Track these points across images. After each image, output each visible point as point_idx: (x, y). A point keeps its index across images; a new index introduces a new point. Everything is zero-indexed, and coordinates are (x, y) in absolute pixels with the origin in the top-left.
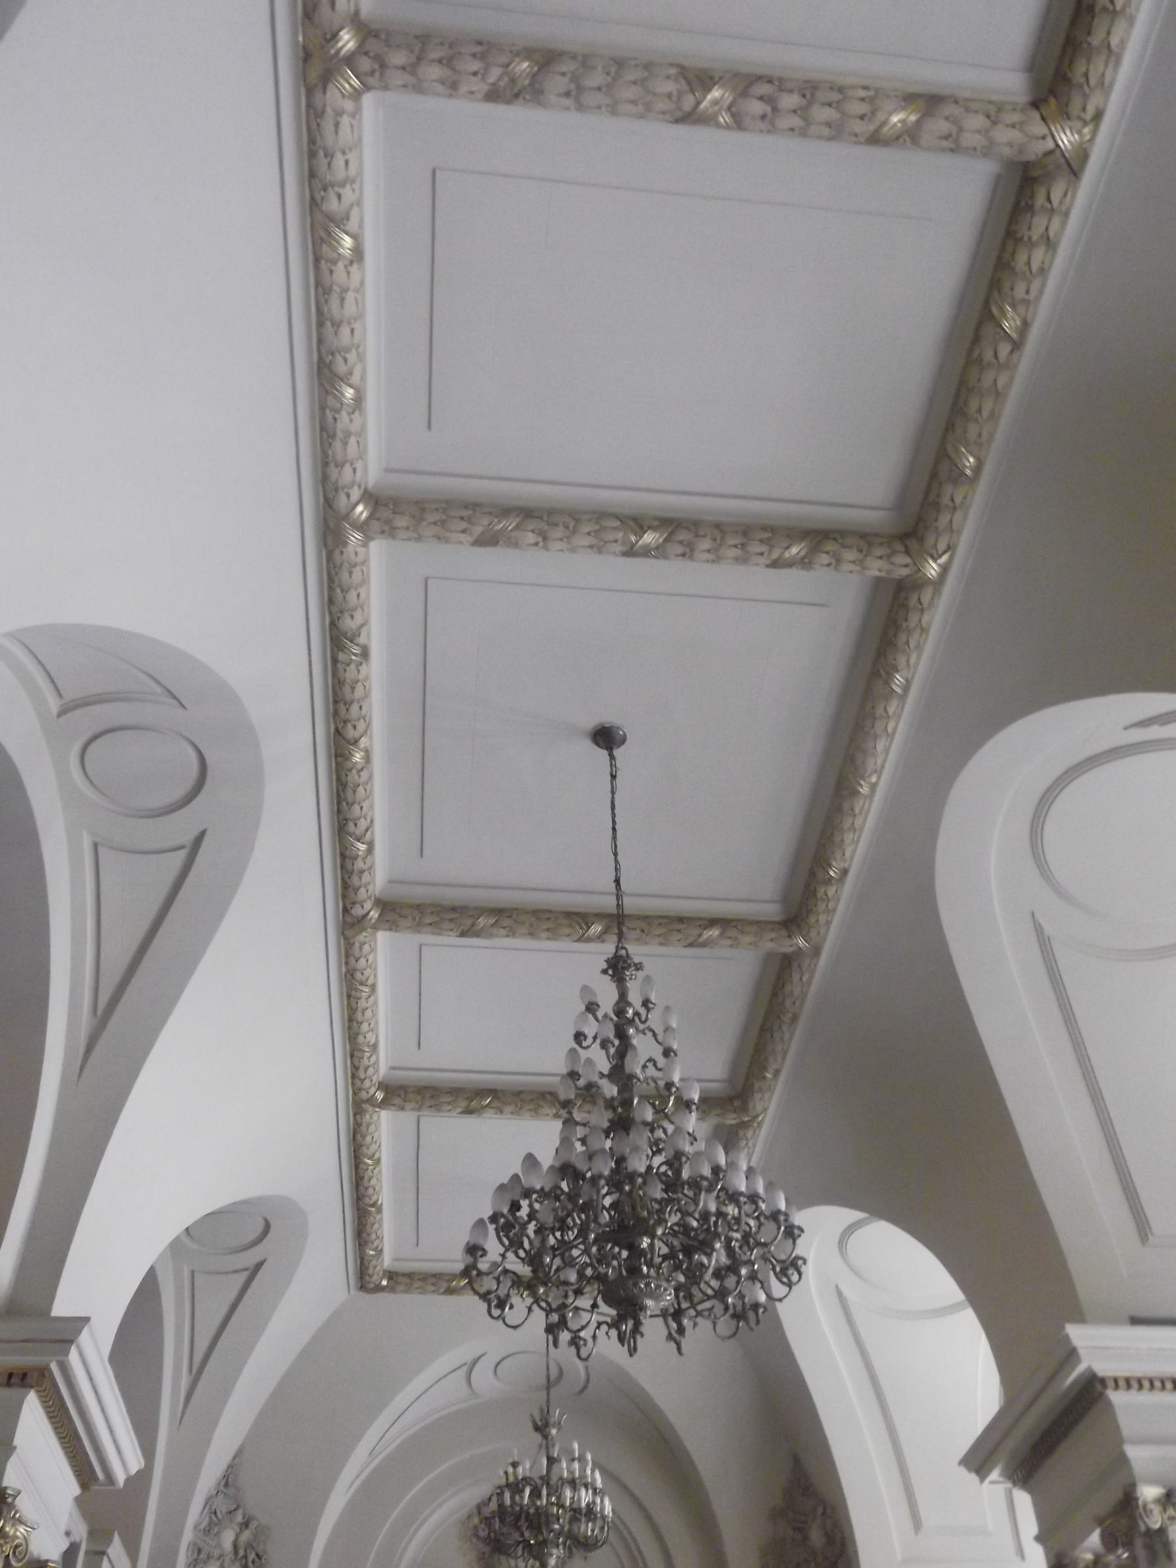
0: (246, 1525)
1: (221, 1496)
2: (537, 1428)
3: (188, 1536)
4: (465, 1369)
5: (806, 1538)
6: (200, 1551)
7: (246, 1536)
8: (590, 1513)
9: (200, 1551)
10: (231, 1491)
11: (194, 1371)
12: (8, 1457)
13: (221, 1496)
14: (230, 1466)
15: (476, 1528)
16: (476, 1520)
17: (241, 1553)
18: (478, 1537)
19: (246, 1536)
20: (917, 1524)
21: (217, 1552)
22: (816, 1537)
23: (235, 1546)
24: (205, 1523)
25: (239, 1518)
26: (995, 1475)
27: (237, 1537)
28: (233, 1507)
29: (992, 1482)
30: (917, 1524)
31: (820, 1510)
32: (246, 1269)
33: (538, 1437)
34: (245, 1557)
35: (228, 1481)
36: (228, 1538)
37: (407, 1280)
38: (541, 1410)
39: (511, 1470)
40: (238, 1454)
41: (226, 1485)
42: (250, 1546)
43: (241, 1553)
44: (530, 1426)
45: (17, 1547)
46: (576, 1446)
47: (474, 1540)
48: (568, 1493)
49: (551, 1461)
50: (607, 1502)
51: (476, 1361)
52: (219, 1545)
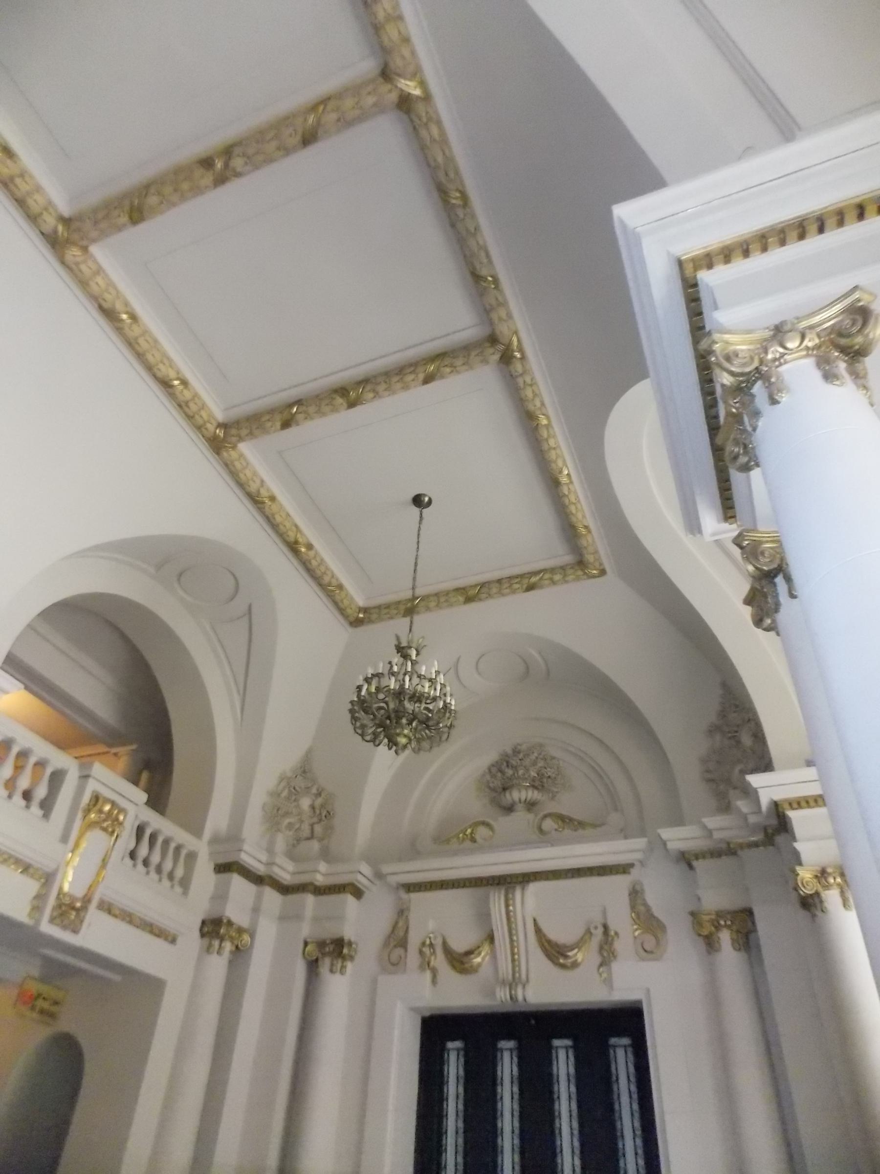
0: (319, 794)
4: (452, 671)
5: (738, 742)
6: (278, 810)
9: (278, 810)
13: (300, 778)
15: (488, 782)
16: (488, 777)
17: (318, 812)
18: (490, 788)
19: (319, 801)
22: (747, 740)
23: (313, 807)
24: (285, 793)
25: (314, 791)
27: (314, 801)
32: (245, 615)
34: (320, 814)
35: (304, 770)
36: (305, 803)
37: (377, 610)
42: (322, 806)
43: (318, 812)
47: (487, 790)
52: (298, 806)
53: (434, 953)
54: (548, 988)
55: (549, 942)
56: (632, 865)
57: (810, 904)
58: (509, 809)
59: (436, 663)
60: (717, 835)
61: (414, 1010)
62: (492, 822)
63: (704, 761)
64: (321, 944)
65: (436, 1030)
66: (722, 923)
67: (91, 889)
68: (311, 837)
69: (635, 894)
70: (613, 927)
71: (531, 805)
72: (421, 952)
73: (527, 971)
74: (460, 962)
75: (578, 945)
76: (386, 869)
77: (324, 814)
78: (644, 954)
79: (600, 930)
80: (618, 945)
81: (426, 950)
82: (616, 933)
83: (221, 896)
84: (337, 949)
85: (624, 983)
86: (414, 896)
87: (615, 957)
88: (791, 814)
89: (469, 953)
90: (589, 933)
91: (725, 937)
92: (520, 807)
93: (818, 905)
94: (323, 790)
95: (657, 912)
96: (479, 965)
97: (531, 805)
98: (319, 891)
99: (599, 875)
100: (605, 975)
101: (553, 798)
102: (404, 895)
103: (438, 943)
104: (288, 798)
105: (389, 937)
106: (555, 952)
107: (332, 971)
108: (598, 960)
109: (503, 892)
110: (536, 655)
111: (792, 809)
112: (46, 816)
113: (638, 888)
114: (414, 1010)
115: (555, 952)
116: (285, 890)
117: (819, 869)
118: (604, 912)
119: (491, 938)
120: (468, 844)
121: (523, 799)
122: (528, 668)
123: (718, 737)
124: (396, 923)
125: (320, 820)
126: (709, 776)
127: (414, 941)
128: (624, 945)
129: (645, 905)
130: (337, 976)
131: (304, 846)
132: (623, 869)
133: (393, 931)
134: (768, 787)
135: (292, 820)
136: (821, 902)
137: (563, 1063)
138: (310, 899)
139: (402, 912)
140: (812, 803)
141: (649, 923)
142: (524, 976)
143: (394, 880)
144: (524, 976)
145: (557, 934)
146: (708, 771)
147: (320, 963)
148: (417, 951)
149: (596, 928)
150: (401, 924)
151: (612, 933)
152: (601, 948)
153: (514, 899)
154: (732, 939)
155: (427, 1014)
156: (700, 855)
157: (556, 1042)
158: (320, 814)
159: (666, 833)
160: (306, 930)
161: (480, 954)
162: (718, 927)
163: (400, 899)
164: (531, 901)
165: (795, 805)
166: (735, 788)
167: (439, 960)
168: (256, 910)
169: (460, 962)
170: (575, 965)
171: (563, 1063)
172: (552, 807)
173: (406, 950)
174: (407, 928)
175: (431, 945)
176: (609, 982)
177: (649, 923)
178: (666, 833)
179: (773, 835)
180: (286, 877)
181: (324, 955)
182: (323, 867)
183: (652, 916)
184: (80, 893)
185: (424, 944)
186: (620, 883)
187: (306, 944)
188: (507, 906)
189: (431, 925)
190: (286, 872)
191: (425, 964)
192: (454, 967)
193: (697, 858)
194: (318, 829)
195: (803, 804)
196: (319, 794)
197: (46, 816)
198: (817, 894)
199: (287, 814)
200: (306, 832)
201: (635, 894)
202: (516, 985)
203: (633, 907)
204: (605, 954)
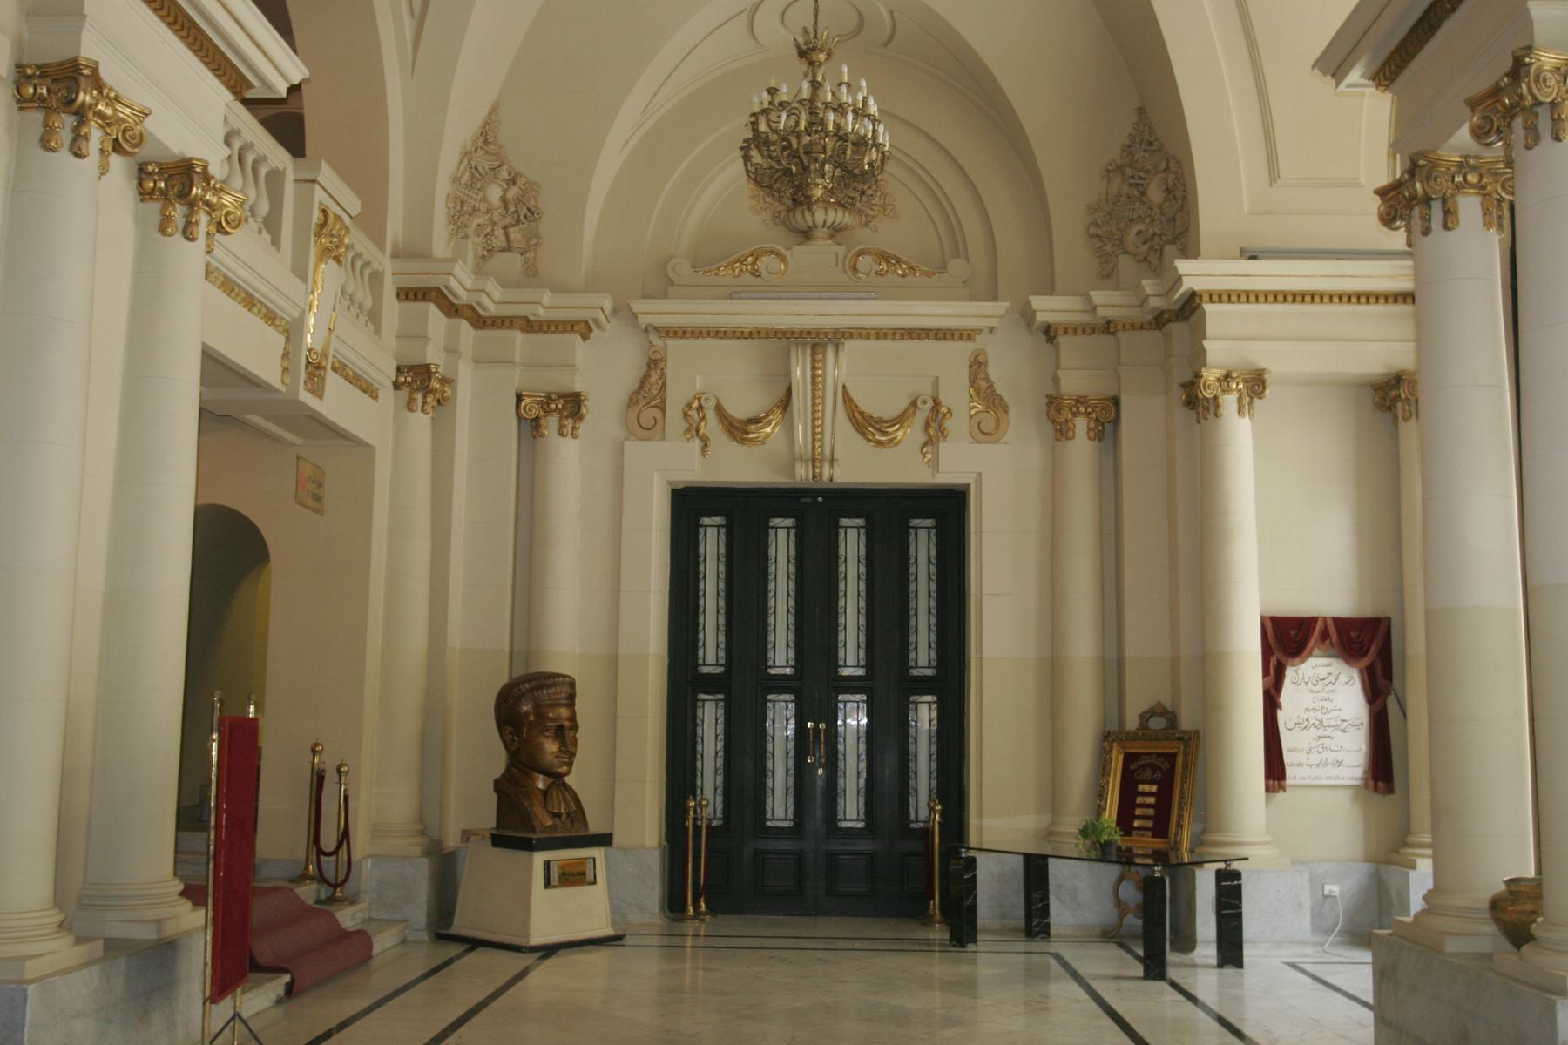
0: (512, 181)
1: (481, 153)
2: (802, 54)
3: (443, 187)
4: (745, 14)
5: (1143, 193)
6: (462, 204)
7: (513, 192)
8: (861, 143)
9: (462, 204)
10: (492, 148)
11: (417, 10)
12: (80, 29)
13: (481, 153)
14: (486, 124)
17: (512, 208)
19: (513, 192)
20: (1273, 174)
21: (483, 206)
22: (1155, 193)
23: (504, 200)
24: (465, 179)
25: (505, 175)
26: (1355, 75)
27: (505, 191)
28: (496, 164)
29: (1349, 86)
30: (1273, 174)
31: (1163, 165)
33: (803, 66)
34: (516, 211)
35: (486, 138)
36: (494, 193)
38: (806, 31)
39: (766, 95)
40: (494, 110)
41: (486, 142)
42: (518, 200)
43: (512, 208)
44: (795, 52)
45: (125, 131)
46: (845, 69)
48: (831, 117)
49: (816, 86)
50: (881, 129)
51: (756, 7)
52: (485, 199)
53: (703, 418)
54: (858, 465)
55: (862, 413)
56: (979, 331)
57: (1196, 403)
58: (806, 235)
59: (864, 84)
60: (1101, 312)
61: (669, 483)
62: (782, 250)
63: (1093, 209)
64: (546, 403)
65: (690, 504)
66: (1082, 409)
67: (327, 344)
68: (508, 248)
69: (977, 366)
70: (946, 401)
71: (835, 232)
72: (686, 415)
73: (833, 447)
74: (738, 430)
75: (901, 420)
76: (638, 306)
77: (523, 212)
78: (980, 436)
79: (930, 404)
80: (948, 424)
81: (693, 413)
82: (949, 411)
83: (413, 334)
84: (572, 405)
85: (953, 465)
86: (672, 344)
87: (944, 437)
88: (1208, 307)
89: (756, 420)
90: (914, 404)
91: (1081, 424)
92: (821, 233)
93: (1212, 409)
94: (518, 174)
95: (999, 389)
96: (768, 435)
97: (835, 232)
98: (530, 326)
99: (938, 339)
100: (929, 456)
101: (866, 224)
102: (657, 342)
103: (710, 405)
104: (470, 186)
105: (637, 392)
106: (866, 425)
107: (561, 434)
108: (922, 438)
109: (809, 352)
110: (884, 11)
111: (1211, 301)
112: (278, 249)
113: (981, 359)
114: (669, 483)
115: (866, 425)
116: (480, 322)
117: (1224, 372)
118: (936, 383)
119: (786, 402)
120: (748, 278)
121: (829, 222)
122: (861, 24)
123: (1117, 180)
124: (646, 377)
125: (518, 221)
126: (1093, 230)
127: (676, 399)
128: (957, 425)
129: (987, 379)
130: (568, 441)
131: (501, 259)
132: (968, 335)
133: (641, 387)
134: (1194, 273)
135: (480, 221)
136: (1217, 406)
137: (852, 543)
138: (518, 337)
139: (654, 364)
140: (1234, 298)
141: (992, 401)
142: (827, 452)
143: (644, 320)
144: (827, 452)
145: (876, 404)
146: (1095, 224)
147: (543, 422)
148: (681, 415)
149: (925, 402)
150: (654, 378)
151: (944, 410)
152: (927, 425)
153: (824, 360)
154: (1089, 429)
155: (681, 486)
156: (1072, 330)
157: (844, 522)
158: (516, 211)
159: (1038, 302)
160: (516, 378)
161: (769, 423)
162: (1076, 414)
163: (651, 345)
164: (841, 367)
165: (1215, 298)
166: (1126, 252)
167: (712, 427)
168: (452, 350)
169: (738, 430)
170: (892, 442)
171: (852, 543)
172: (865, 237)
173: (663, 411)
174: (664, 385)
175: (700, 407)
176: (935, 465)
177: (992, 401)
178: (1038, 302)
179: (1169, 321)
180: (491, 309)
181: (548, 412)
182: (547, 298)
183: (995, 394)
184: (319, 348)
185: (689, 406)
186: (961, 352)
187: (519, 398)
188: (814, 368)
189: (699, 384)
190: (493, 300)
191: (693, 430)
192: (733, 437)
193: (1066, 332)
194: (515, 234)
195: (1225, 298)
196: (512, 181)
197: (278, 249)
198: (1216, 398)
199: (475, 210)
200: (499, 239)
201: (977, 366)
202: (821, 461)
203: (972, 382)
204: (932, 432)
